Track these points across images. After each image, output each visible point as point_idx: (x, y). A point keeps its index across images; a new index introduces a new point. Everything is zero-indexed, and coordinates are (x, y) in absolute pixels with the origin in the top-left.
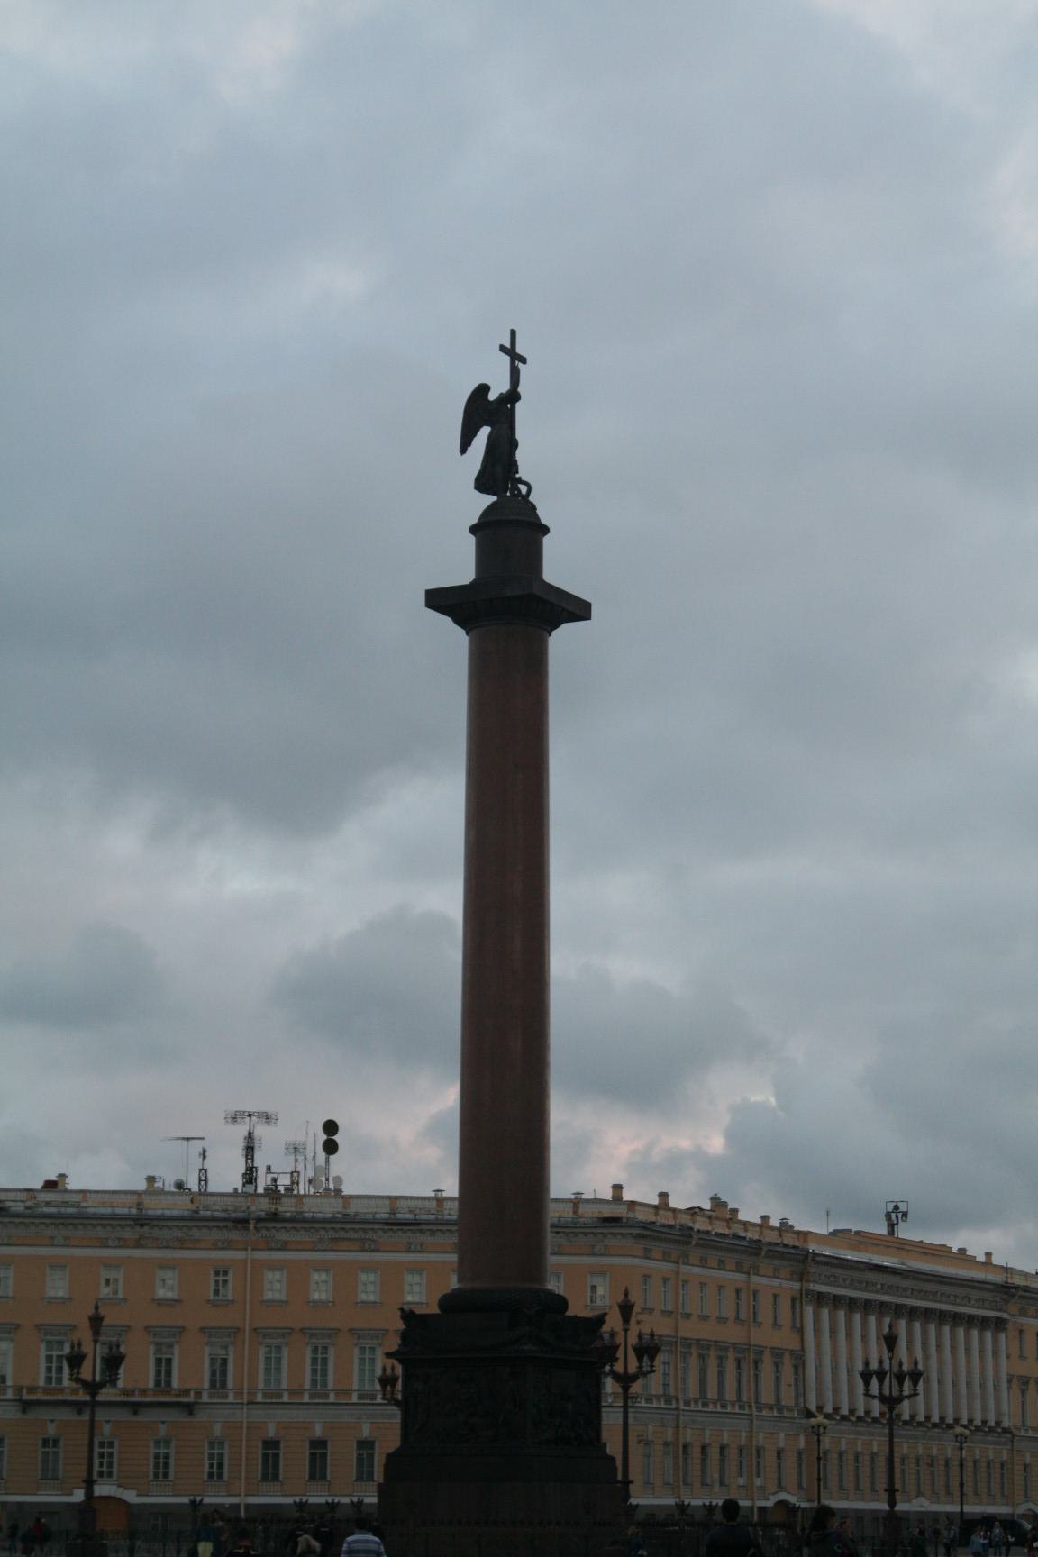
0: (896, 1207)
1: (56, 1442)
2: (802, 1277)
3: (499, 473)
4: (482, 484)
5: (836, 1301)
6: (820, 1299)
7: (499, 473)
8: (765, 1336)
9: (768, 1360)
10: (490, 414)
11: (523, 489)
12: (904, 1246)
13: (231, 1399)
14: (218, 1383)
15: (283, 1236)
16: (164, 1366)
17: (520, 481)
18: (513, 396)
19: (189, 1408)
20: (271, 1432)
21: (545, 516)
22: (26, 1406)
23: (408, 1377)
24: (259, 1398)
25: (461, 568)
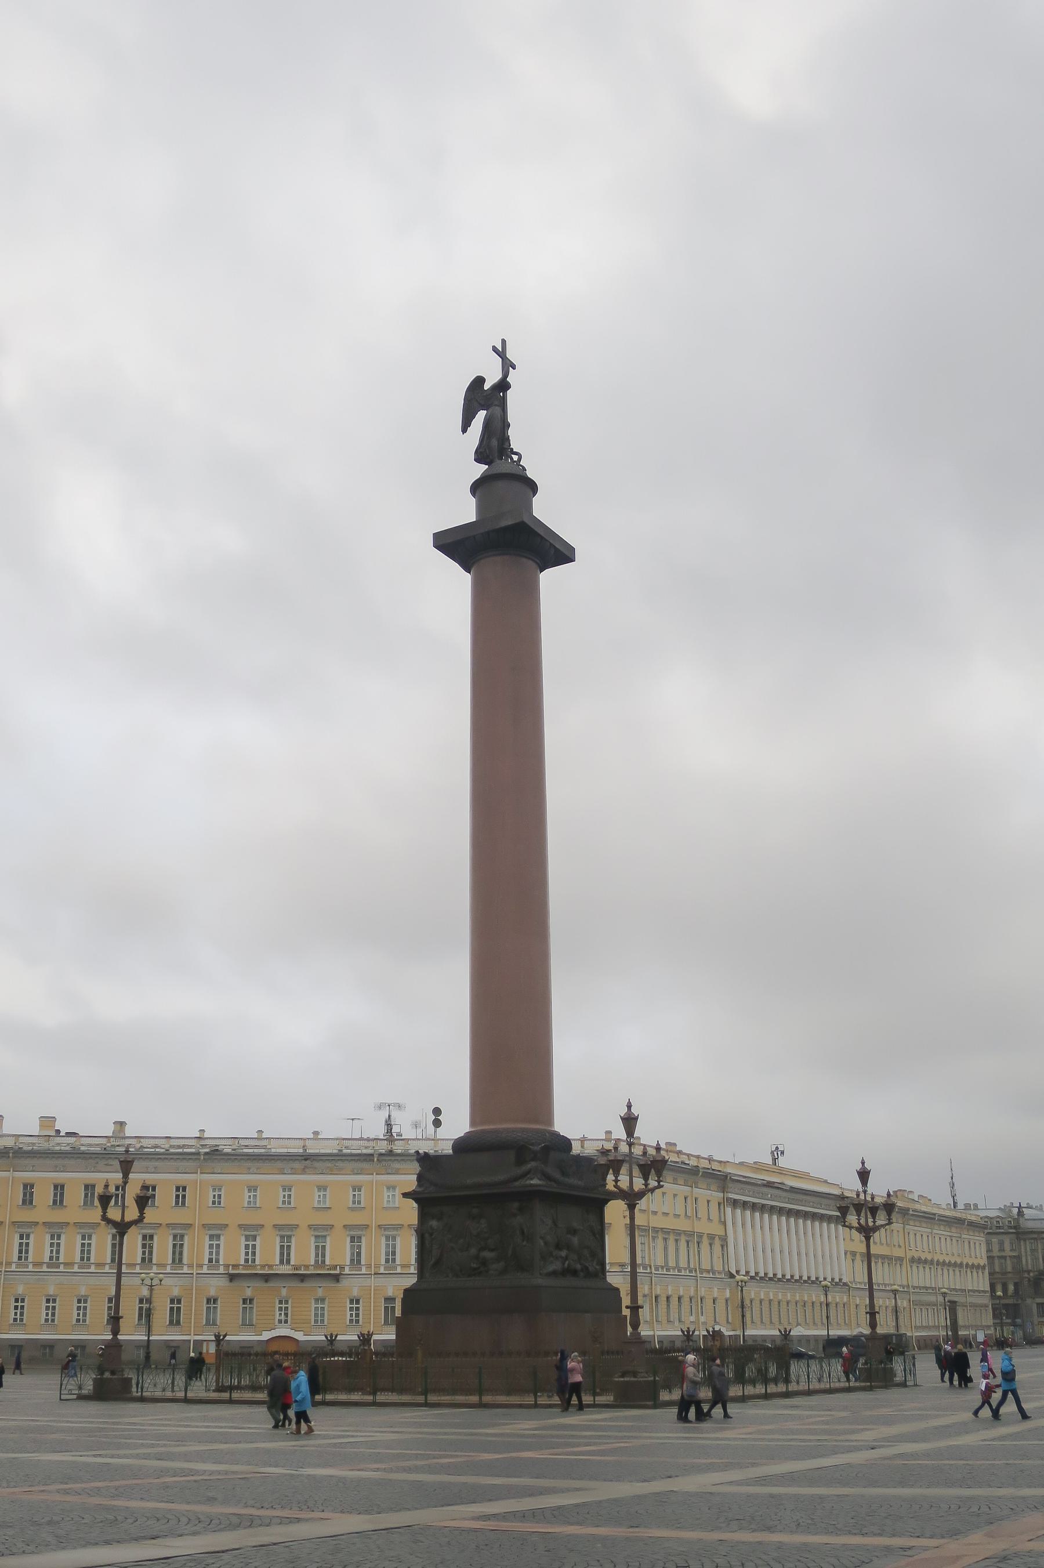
0: (777, 1148)
1: (251, 1301)
2: (723, 1189)
3: (495, 446)
4: (481, 456)
5: (745, 1205)
6: (735, 1203)
7: (495, 446)
8: (703, 1227)
9: (705, 1242)
10: (486, 400)
11: (515, 458)
12: (782, 1172)
14: (356, 1261)
15: (396, 1165)
16: (321, 1251)
18: (503, 386)
19: (336, 1278)
22: (232, 1278)
23: (423, 1216)
24: (382, 1271)
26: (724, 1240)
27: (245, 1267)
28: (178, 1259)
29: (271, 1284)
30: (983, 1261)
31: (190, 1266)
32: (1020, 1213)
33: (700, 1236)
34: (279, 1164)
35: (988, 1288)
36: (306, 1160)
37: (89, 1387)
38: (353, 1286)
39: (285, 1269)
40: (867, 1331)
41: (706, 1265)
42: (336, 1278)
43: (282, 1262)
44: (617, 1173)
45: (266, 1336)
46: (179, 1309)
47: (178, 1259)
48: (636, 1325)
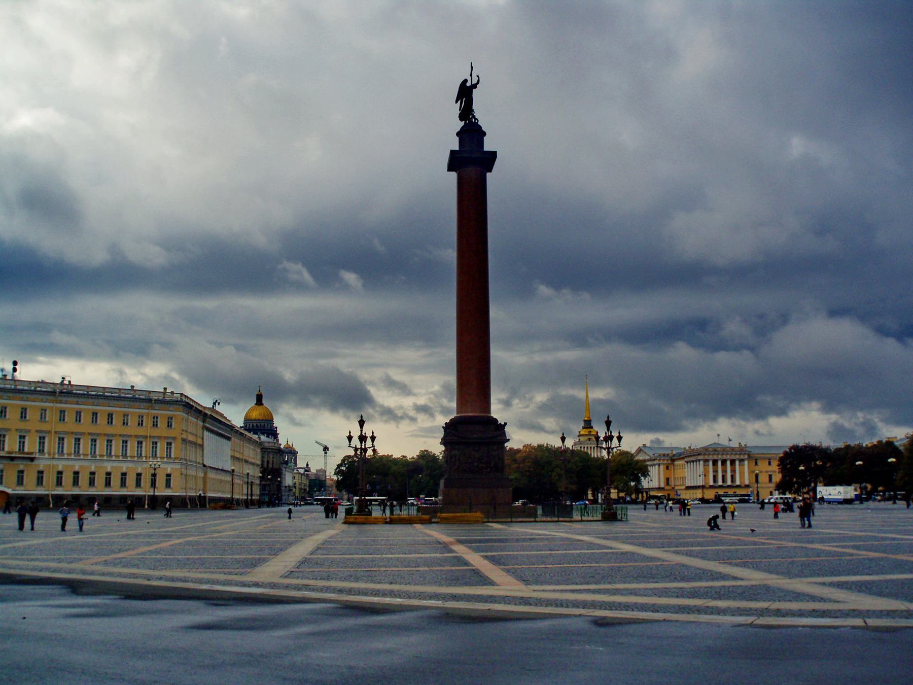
2: (204, 421)
3: (466, 113)
4: (462, 117)
10: (465, 93)
12: (217, 412)
14: (41, 451)
16: (22, 444)
18: (474, 86)
19: (32, 459)
20: (60, 469)
24: (57, 456)
26: (202, 446)
30: (259, 462)
38: (41, 464)
40: (229, 496)
42: (32, 459)
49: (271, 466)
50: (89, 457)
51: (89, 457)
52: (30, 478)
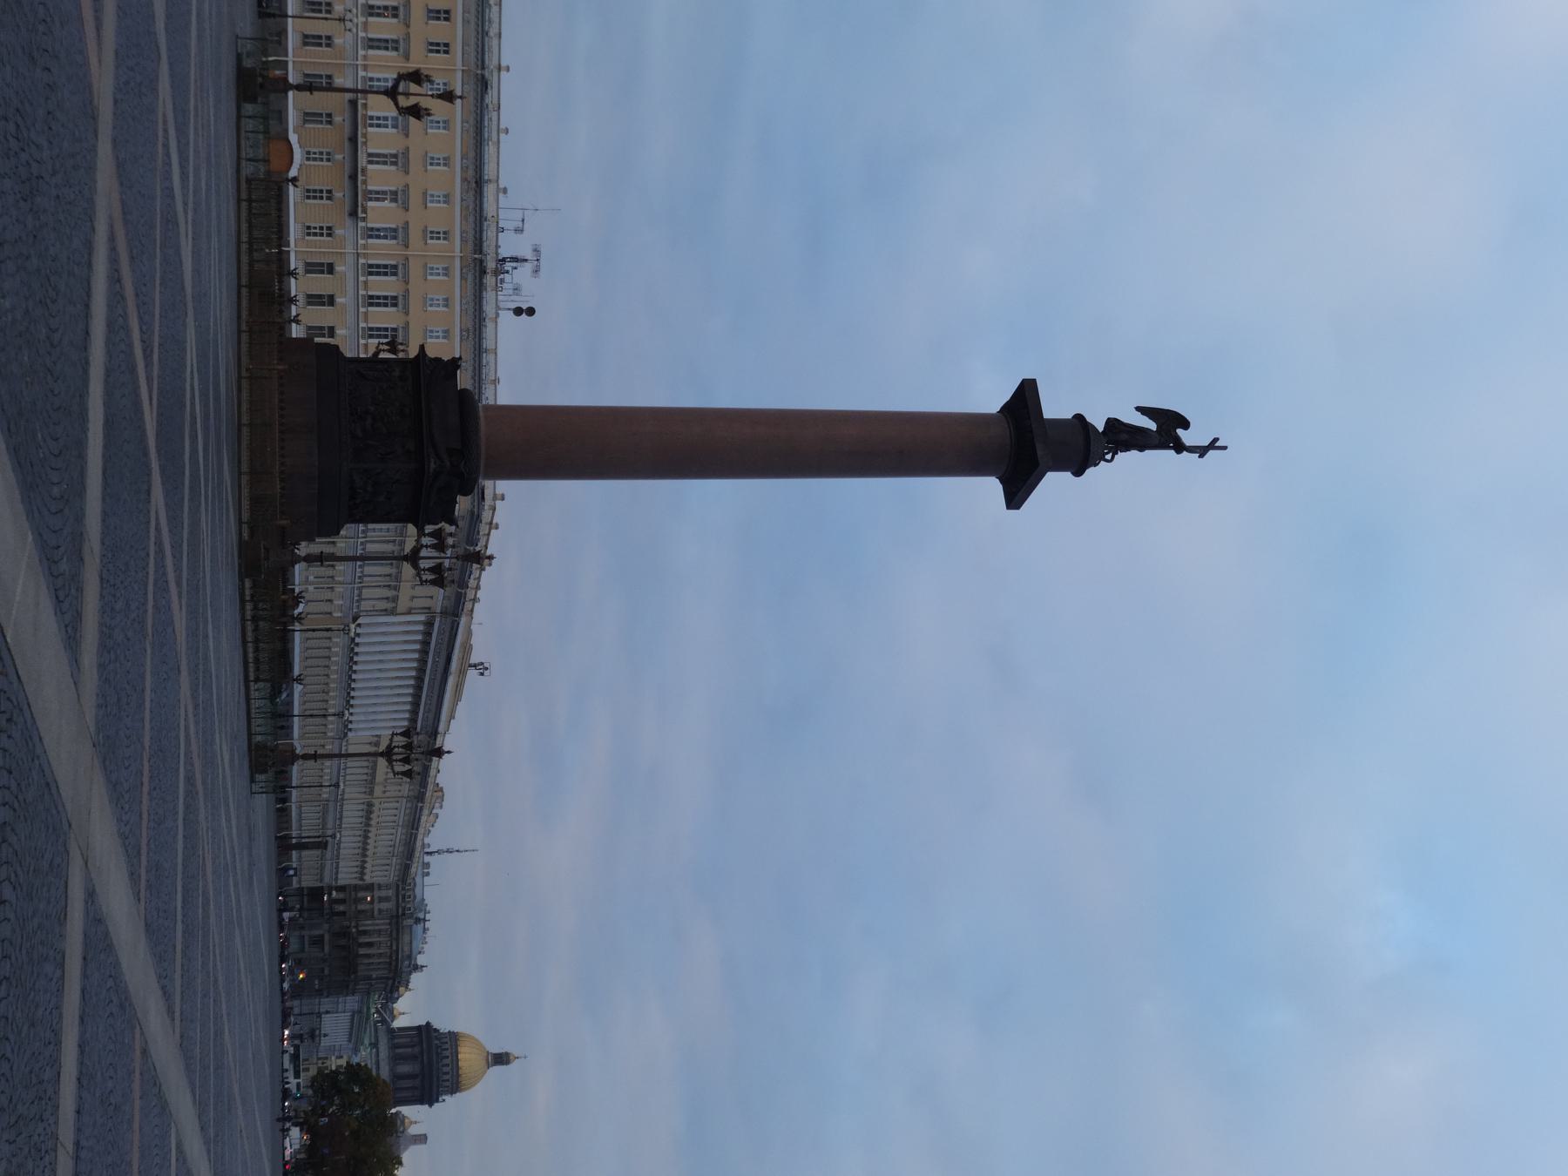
1: (330, 123)
2: (444, 613)
3: (1120, 437)
4: (1112, 424)
5: (428, 634)
7: (1120, 437)
9: (390, 593)
10: (1165, 430)
11: (1108, 457)
12: (462, 673)
13: (361, 242)
14: (372, 233)
15: (470, 278)
16: (379, 196)
17: (1115, 453)
18: (1180, 447)
19: (353, 214)
21: (1090, 471)
23: (404, 363)
24: (362, 261)
25: (1054, 407)
26: (392, 612)
27: (365, 116)
28: (372, 44)
29: (347, 143)
30: (368, 879)
31: (365, 58)
32: (418, 921)
33: (396, 588)
34: (472, 154)
35: (341, 883)
36: (477, 182)
37: (248, 63)
39: (362, 160)
41: (366, 593)
43: (370, 155)
44: (433, 546)
45: (293, 138)
46: (320, 45)
47: (372, 44)
48: (309, 559)
49: (362, 951)
50: (362, 325)
51: (362, 325)
52: (320, 212)
